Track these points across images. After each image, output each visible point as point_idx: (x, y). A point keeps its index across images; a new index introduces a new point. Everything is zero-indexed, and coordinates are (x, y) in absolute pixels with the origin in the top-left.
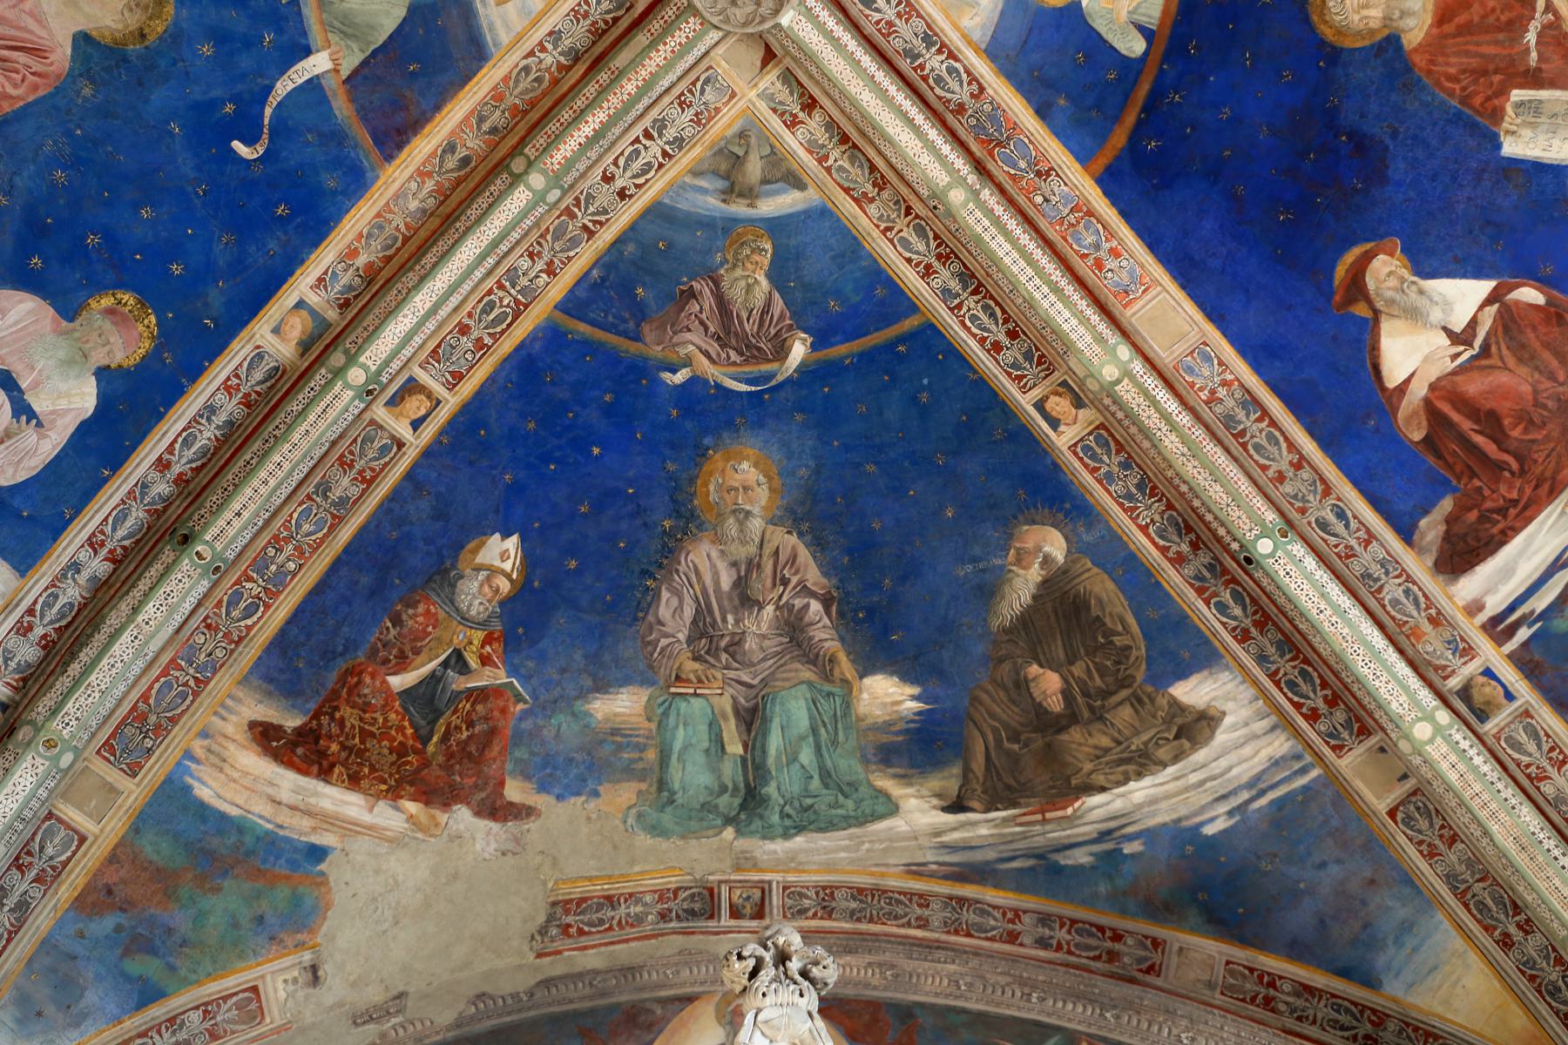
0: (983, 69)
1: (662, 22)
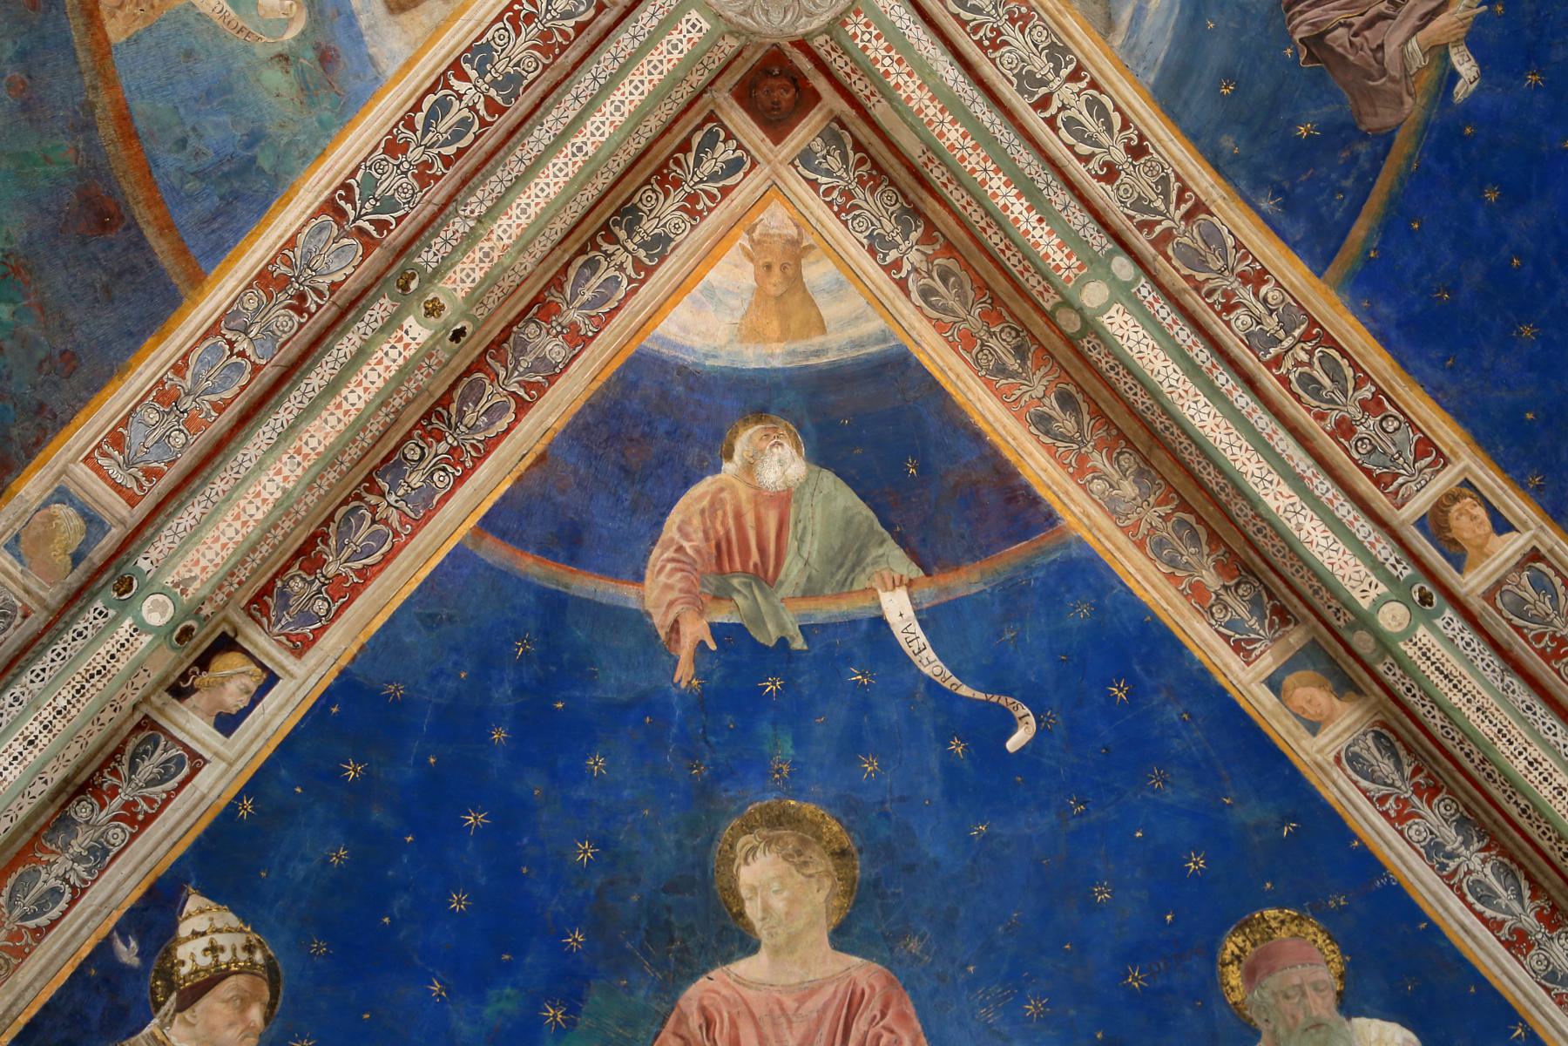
1: (855, 77)
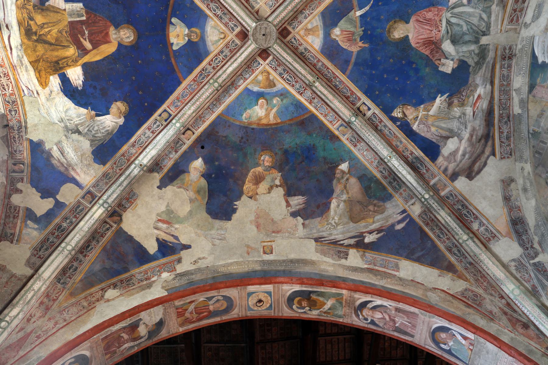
0: (208, 12)
